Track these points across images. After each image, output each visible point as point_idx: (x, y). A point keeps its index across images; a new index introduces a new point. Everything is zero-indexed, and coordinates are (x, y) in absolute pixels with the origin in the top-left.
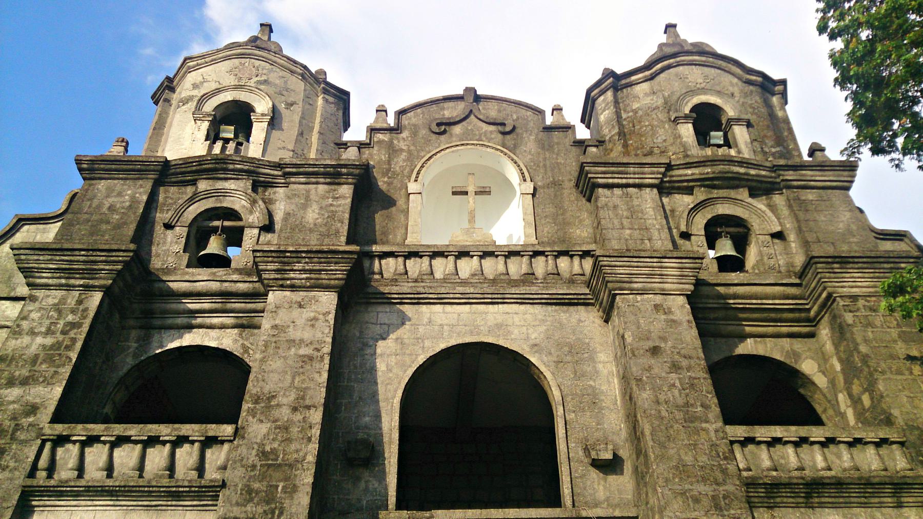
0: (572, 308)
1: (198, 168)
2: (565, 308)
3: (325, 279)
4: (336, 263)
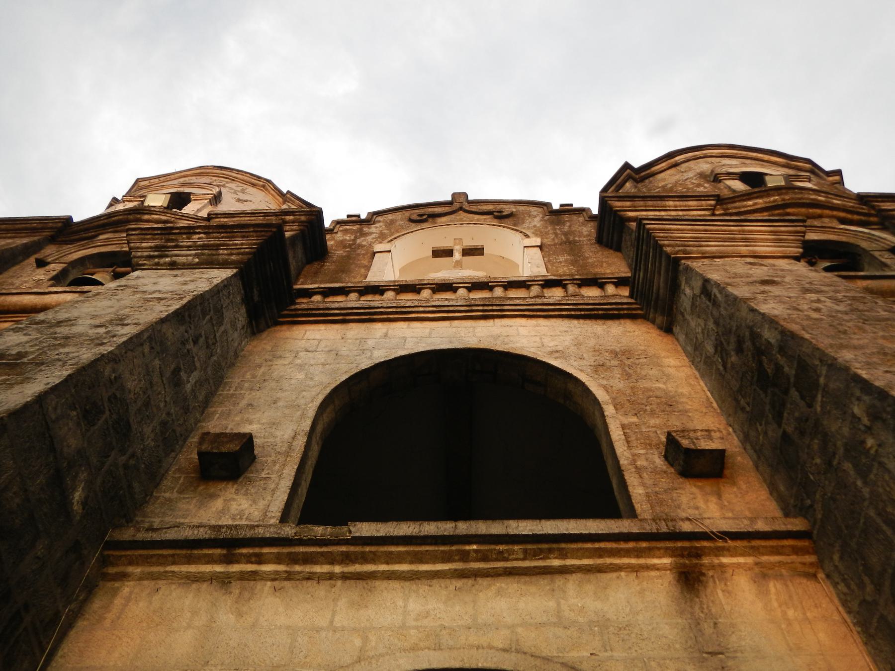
0: (610, 323)
1: (106, 221)
2: (600, 322)
3: (223, 254)
4: (243, 237)
